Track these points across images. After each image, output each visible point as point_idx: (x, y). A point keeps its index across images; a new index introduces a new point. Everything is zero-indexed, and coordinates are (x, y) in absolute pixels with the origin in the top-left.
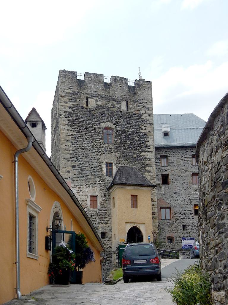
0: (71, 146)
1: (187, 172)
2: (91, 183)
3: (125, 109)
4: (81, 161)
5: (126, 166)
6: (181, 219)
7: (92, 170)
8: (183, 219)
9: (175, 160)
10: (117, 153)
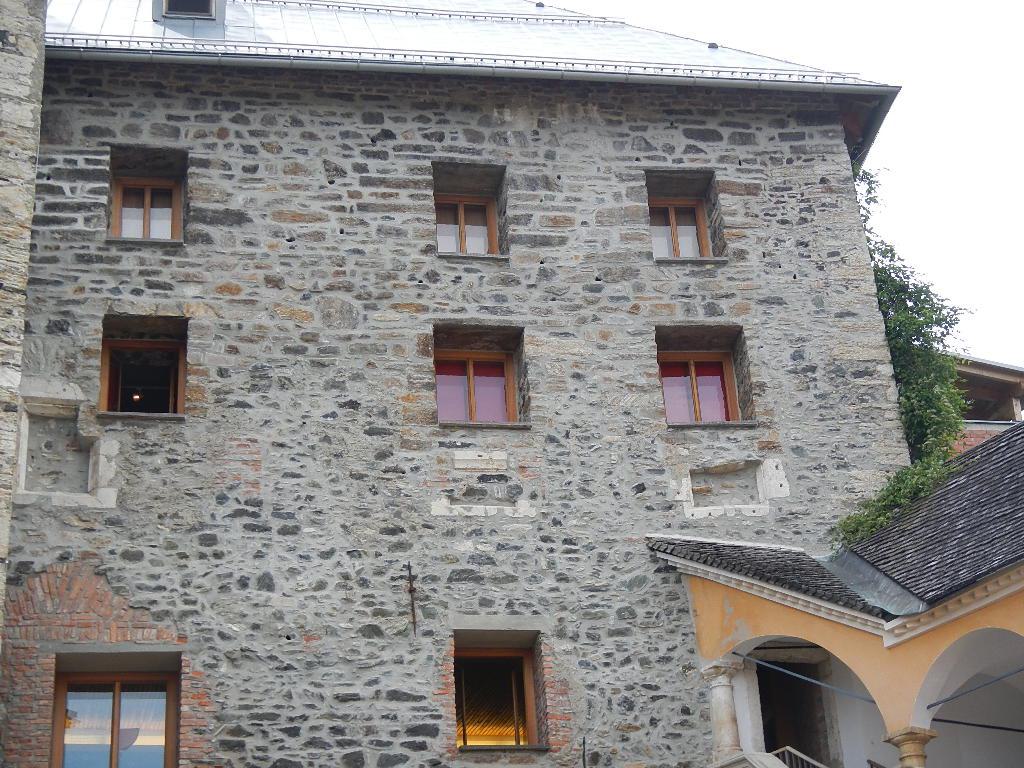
1: (384, 315)
9: (262, 196)
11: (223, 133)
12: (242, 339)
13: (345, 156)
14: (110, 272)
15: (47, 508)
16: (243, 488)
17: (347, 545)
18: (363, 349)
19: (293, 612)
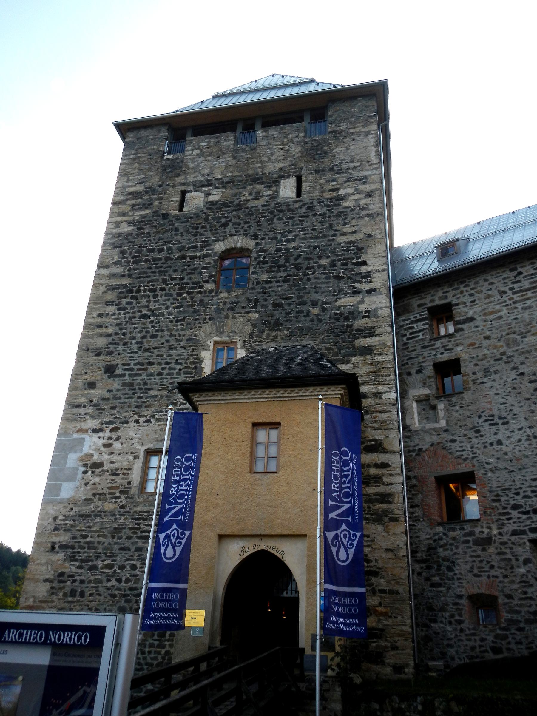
0: (113, 314)
2: (154, 412)
3: (291, 196)
4: (135, 350)
5: (283, 345)
6: (524, 517)
7: (165, 372)
8: (532, 515)
10: (256, 312)
11: (462, 292)
12: (479, 360)
13: (505, 286)
14: (432, 349)
15: (424, 430)
16: (486, 412)
17: (527, 424)
18: (523, 353)
19: (510, 451)
